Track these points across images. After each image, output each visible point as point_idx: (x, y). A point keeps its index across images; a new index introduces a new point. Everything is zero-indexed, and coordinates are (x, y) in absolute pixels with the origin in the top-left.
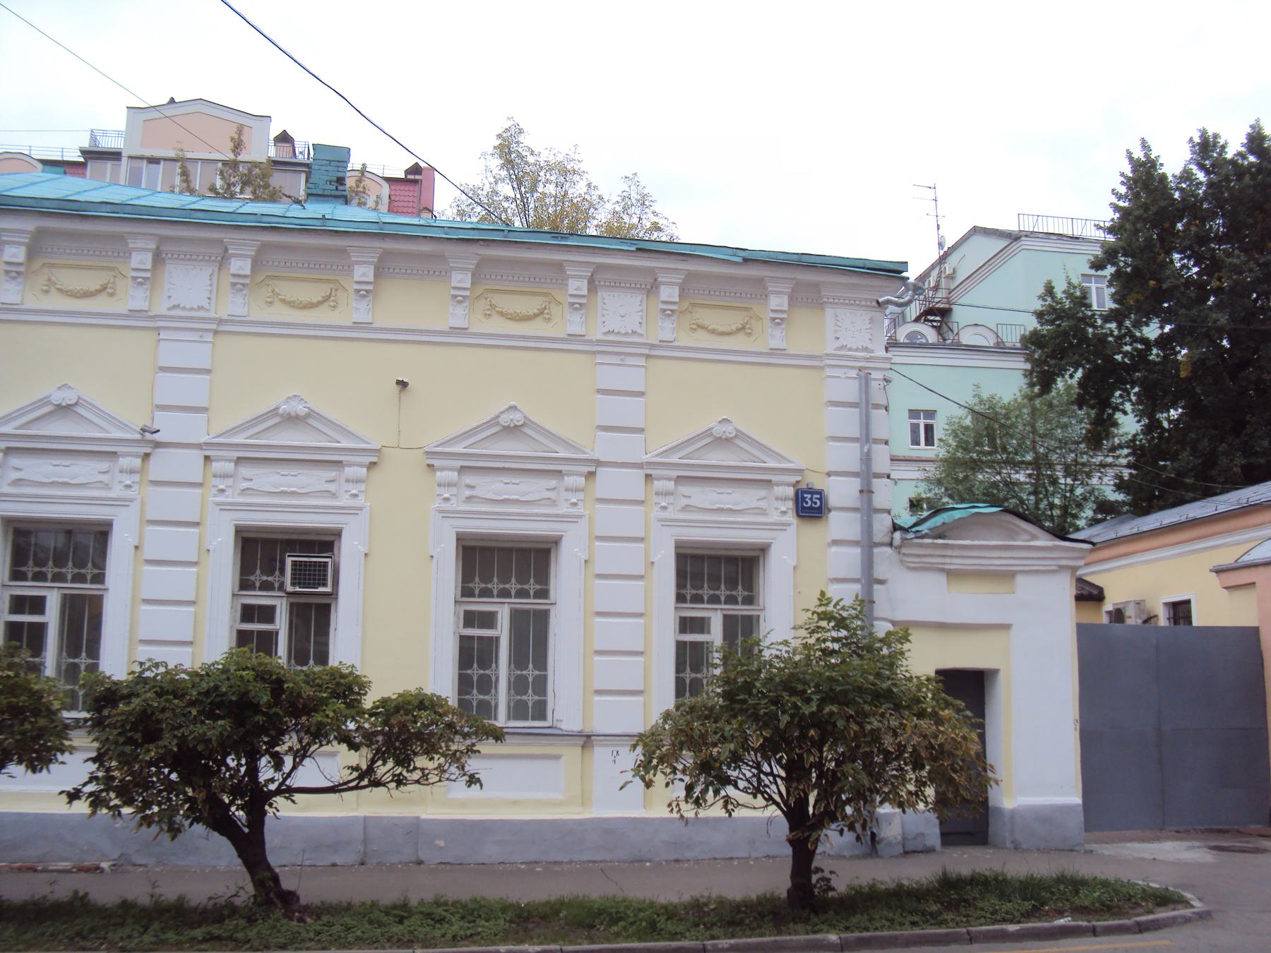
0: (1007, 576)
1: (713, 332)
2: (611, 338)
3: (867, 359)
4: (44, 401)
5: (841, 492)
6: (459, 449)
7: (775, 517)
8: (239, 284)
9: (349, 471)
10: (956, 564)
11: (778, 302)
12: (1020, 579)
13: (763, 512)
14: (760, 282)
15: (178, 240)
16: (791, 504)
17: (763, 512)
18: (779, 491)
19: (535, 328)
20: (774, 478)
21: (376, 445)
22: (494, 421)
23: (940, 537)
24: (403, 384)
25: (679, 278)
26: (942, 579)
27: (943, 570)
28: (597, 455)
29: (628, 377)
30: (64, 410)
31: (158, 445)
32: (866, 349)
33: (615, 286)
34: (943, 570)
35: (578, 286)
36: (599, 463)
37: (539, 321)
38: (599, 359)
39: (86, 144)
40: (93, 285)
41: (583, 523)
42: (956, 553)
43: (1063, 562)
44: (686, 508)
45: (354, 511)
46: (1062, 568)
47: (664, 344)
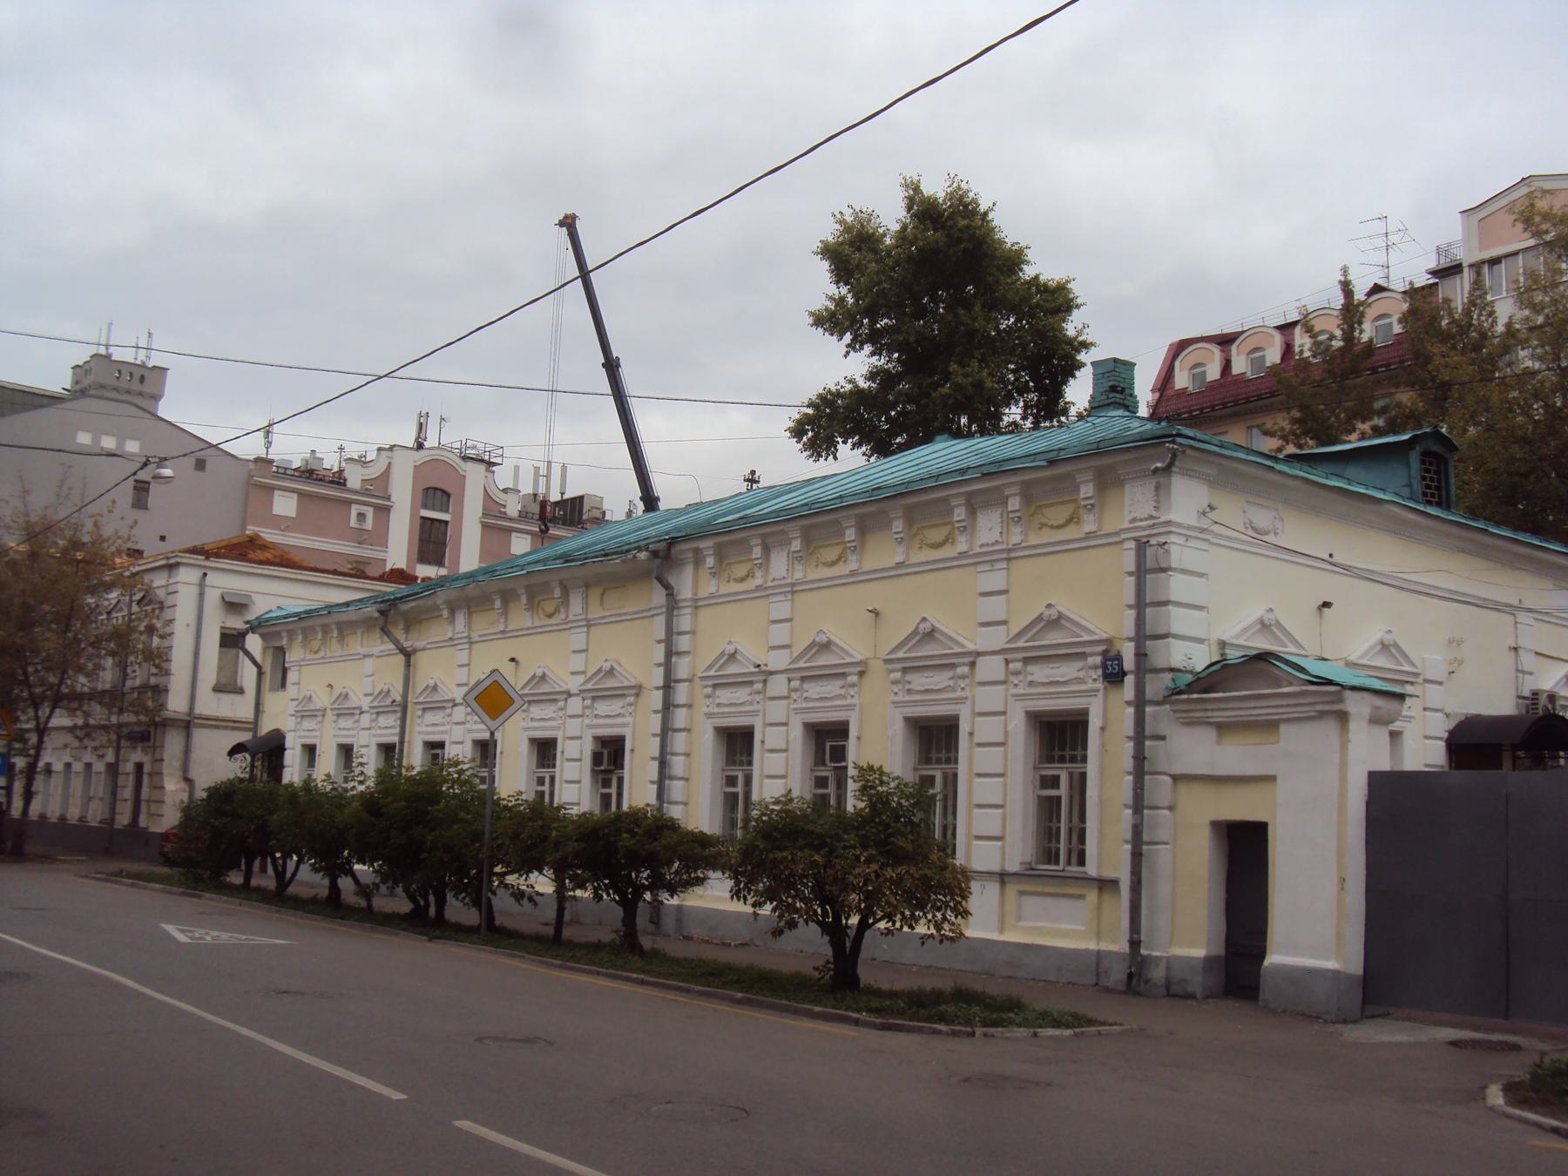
0: (1269, 726)
1: (1052, 527)
2: (985, 549)
3: (1152, 526)
4: (723, 654)
5: (1128, 653)
6: (900, 655)
7: (1090, 685)
8: (797, 558)
9: (960, 670)
10: (1219, 716)
11: (1087, 490)
12: (1283, 728)
13: (1081, 681)
14: (1069, 476)
15: (816, 526)
16: (1100, 672)
17: (1081, 681)
18: (1090, 660)
19: (947, 552)
20: (1088, 650)
21: (859, 658)
22: (915, 633)
23: (1206, 691)
24: (876, 613)
25: (1016, 490)
26: (1209, 734)
27: (1210, 724)
28: (971, 647)
29: (995, 580)
30: (732, 657)
31: (772, 673)
32: (1151, 517)
33: (987, 505)
34: (1210, 724)
35: (960, 513)
36: (979, 654)
37: (948, 546)
38: (980, 568)
39: (1433, 265)
40: (834, 557)
41: (969, 702)
42: (1214, 706)
43: (1319, 707)
44: (1031, 684)
45: (851, 707)
46: (1322, 715)
47: (1016, 547)
